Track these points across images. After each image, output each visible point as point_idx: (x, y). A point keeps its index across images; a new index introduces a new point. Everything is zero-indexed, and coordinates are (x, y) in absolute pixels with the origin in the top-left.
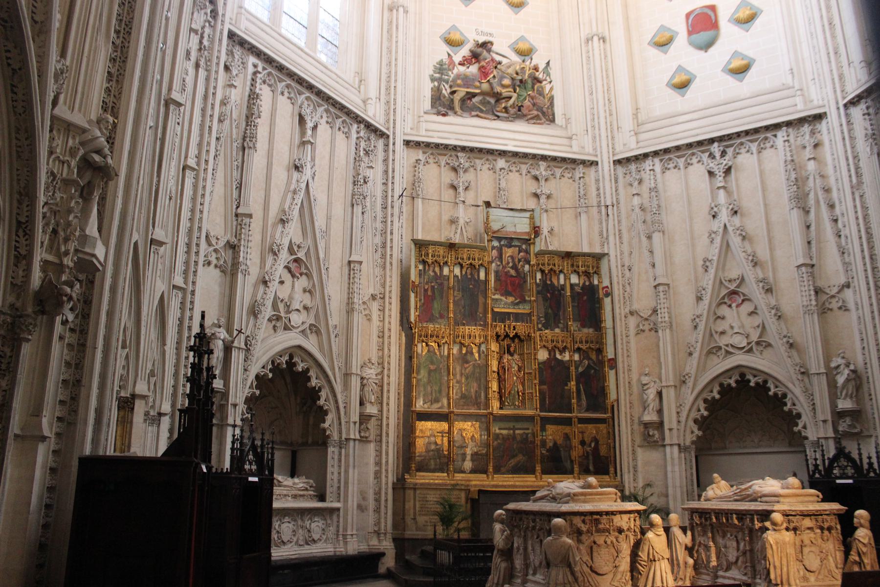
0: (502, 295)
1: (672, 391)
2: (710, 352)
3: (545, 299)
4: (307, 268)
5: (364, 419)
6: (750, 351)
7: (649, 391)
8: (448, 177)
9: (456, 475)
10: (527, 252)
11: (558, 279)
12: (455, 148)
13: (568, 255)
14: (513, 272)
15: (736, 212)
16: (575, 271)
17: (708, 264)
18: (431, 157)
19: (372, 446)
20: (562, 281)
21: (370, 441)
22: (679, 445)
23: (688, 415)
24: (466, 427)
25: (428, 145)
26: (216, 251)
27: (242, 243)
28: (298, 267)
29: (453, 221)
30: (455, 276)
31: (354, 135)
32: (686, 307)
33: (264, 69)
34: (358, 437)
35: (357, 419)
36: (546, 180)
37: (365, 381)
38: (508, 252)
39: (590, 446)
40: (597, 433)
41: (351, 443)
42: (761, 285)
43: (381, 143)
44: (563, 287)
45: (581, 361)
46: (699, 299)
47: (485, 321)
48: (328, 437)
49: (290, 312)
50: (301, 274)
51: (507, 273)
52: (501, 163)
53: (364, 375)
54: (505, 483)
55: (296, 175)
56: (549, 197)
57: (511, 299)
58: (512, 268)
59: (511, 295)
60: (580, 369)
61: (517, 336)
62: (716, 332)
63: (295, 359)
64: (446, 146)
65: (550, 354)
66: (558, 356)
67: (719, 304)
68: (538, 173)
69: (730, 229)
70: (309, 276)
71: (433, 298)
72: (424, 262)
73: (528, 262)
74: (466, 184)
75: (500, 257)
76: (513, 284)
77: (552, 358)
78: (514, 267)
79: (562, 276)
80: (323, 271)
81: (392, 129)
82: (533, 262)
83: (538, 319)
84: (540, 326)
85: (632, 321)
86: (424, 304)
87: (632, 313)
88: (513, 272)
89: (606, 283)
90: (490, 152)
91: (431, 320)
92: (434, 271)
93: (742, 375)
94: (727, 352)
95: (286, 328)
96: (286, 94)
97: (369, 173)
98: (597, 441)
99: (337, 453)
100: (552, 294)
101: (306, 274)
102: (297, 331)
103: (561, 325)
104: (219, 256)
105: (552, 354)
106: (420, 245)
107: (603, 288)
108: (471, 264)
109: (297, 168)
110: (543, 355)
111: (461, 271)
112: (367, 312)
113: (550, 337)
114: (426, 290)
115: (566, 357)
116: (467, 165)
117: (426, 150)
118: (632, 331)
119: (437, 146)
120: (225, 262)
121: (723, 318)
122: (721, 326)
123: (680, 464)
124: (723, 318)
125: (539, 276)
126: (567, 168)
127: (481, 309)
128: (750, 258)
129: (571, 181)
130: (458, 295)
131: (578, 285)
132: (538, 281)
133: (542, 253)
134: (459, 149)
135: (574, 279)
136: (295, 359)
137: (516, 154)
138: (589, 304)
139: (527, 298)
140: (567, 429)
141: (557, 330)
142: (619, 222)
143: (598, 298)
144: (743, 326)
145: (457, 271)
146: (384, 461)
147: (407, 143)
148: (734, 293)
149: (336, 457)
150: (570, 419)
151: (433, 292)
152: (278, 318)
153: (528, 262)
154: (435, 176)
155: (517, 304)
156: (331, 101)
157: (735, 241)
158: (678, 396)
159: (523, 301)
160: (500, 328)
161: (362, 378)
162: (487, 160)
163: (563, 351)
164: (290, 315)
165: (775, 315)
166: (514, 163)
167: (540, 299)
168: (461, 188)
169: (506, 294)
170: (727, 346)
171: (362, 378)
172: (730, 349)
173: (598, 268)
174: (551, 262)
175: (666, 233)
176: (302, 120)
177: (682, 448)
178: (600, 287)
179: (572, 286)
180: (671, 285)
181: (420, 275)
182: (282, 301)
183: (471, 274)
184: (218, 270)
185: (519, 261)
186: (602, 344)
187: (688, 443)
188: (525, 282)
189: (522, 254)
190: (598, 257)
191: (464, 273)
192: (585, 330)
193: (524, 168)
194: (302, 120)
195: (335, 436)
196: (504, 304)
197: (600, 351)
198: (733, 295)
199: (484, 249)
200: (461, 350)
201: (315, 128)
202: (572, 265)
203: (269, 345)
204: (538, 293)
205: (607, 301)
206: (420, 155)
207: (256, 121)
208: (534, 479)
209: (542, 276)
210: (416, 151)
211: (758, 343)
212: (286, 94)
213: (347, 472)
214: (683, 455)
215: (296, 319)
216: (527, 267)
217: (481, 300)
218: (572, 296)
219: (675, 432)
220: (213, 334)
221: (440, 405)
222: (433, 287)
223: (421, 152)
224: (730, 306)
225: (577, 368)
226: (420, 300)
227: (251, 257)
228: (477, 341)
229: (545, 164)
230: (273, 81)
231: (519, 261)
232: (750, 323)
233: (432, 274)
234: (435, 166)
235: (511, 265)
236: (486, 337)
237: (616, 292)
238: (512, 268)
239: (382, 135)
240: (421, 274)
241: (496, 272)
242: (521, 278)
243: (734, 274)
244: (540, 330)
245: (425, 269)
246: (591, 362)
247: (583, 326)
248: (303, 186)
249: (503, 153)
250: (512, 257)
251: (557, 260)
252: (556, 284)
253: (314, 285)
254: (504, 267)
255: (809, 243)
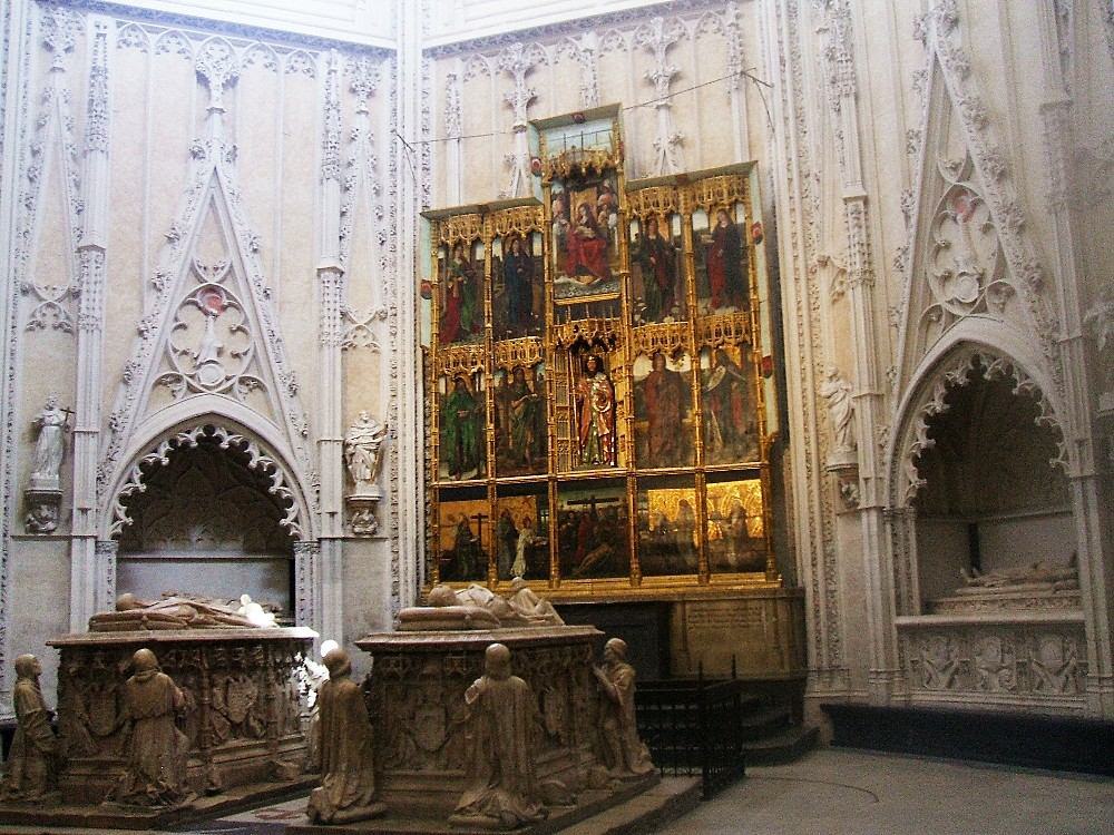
0: (570, 276)
1: (867, 404)
2: (927, 322)
3: (646, 267)
4: (229, 296)
5: (351, 506)
6: (982, 308)
7: (835, 409)
8: (504, 87)
9: (502, 583)
10: (612, 191)
11: (670, 227)
12: (506, 39)
13: (683, 181)
14: (588, 232)
15: (955, 22)
16: (698, 207)
17: (914, 142)
18: (476, 63)
19: (388, 544)
20: (677, 231)
21: (384, 539)
22: (880, 509)
23: (896, 453)
24: (515, 504)
25: (463, 47)
26: (50, 305)
27: (85, 287)
28: (211, 296)
29: (509, 164)
30: (494, 259)
31: (322, 69)
32: (895, 235)
33: (119, 24)
34: (339, 533)
35: (338, 507)
36: (670, 47)
37: (351, 450)
38: (578, 200)
39: (729, 520)
40: (743, 496)
41: (326, 545)
42: (990, 165)
43: (387, 62)
44: (679, 241)
45: (712, 371)
46: (907, 218)
47: (543, 325)
48: (296, 537)
49: (199, 367)
50: (224, 308)
51: (580, 238)
52: (589, 39)
53: (349, 440)
54: (575, 594)
55: (195, 165)
56: (674, 78)
57: (586, 279)
58: (587, 225)
59: (587, 272)
60: (711, 385)
61: (581, 343)
62: (175, 351)
63: (218, 432)
64: (492, 41)
65: (654, 366)
66: (670, 367)
67: (941, 220)
68: (650, 39)
69: (942, 60)
70: (238, 307)
71: (461, 302)
72: (444, 246)
73: (613, 208)
74: (529, 96)
75: (566, 205)
76: (588, 254)
77: (660, 372)
78: (592, 223)
79: (676, 222)
80: (255, 296)
81: (399, 40)
82: (623, 206)
83: (634, 306)
84: (637, 318)
85: (823, 280)
86: (446, 315)
87: (824, 263)
88: (588, 232)
89: (757, 218)
90: (565, 28)
91: (460, 336)
92: (461, 257)
93: (976, 360)
94: (953, 317)
95: (192, 389)
96: (173, 47)
97: (362, 123)
98: (743, 514)
99: (307, 560)
100: (660, 257)
101: (230, 305)
102: (214, 392)
103: (675, 310)
104: (57, 311)
105: (659, 363)
106: (436, 219)
107: (753, 227)
108: (514, 233)
109: (195, 155)
110: (643, 368)
111: (503, 249)
112: (369, 341)
113: (649, 336)
114: (449, 291)
115: (686, 364)
116: (527, 63)
117: (465, 55)
118: (825, 297)
119: (478, 43)
120: (68, 318)
121: (948, 246)
122: (947, 263)
123: (882, 550)
124: (948, 246)
125: (634, 229)
126: (710, 15)
127: (536, 306)
128: (973, 113)
129: (719, 35)
130: (500, 288)
131: (702, 231)
132: (633, 239)
133: (632, 190)
134: (514, 38)
135: (700, 222)
136: (218, 432)
137: (608, 19)
138: (728, 265)
139: (614, 273)
140: (690, 494)
141: (668, 320)
142: (797, 92)
143: (746, 248)
144: (975, 259)
145: (497, 250)
146: (402, 568)
147: (432, 53)
148: (958, 192)
149: (307, 567)
150: (691, 475)
151: (460, 291)
152: (178, 379)
153: (613, 208)
154: (483, 93)
155: (599, 285)
156: (259, 32)
157: (952, 80)
158: (880, 415)
159: (607, 279)
160: (567, 334)
161: (346, 446)
162: (567, 41)
163: (677, 354)
164: (199, 371)
165: (1012, 225)
166: (613, 33)
167: (638, 269)
168: (519, 105)
169: (578, 271)
170: (951, 302)
171: (346, 446)
172: (956, 311)
173: (742, 191)
174: (651, 201)
175: (864, 92)
176: (202, 79)
177: (890, 516)
178: (748, 227)
179: (695, 236)
180: (873, 199)
181: (440, 269)
182: (185, 353)
183: (520, 250)
184: (59, 332)
185: (599, 209)
186: (749, 331)
187: (901, 503)
188: (611, 244)
189: (602, 197)
190: (740, 175)
191: (507, 250)
192: (718, 313)
193: (628, 37)
194: (202, 79)
195: (306, 538)
196: (578, 290)
197: (745, 346)
198: (953, 200)
199: (533, 203)
200: (505, 379)
201: (231, 83)
202: (694, 198)
203: (154, 419)
204: (634, 259)
205: (760, 249)
206: (457, 66)
207: (99, 109)
208: (628, 585)
209: (641, 230)
210: (451, 60)
211: (995, 289)
212: (173, 47)
213: (320, 588)
214: (888, 527)
215: (208, 375)
216: (613, 218)
217: (536, 289)
218: (697, 257)
219: (872, 483)
220: (42, 420)
221: (475, 472)
222: (460, 283)
223: (458, 60)
224: (955, 220)
225: (703, 383)
226: (441, 308)
227: (110, 301)
228: (529, 361)
229: (661, 19)
230: (141, 36)
231: (599, 209)
232: (985, 248)
233: (458, 262)
234: (483, 76)
235: (585, 219)
236: (543, 352)
237: (787, 228)
238: (587, 225)
239: (385, 53)
240: (441, 266)
241: (561, 239)
242: (604, 237)
243: (958, 155)
244: (635, 324)
245: (447, 254)
246: (731, 369)
247: (717, 305)
248: (207, 178)
249: (586, 24)
250: (585, 206)
251: (661, 194)
252: (666, 238)
253: (246, 321)
254: (573, 227)
255: (1064, 54)
